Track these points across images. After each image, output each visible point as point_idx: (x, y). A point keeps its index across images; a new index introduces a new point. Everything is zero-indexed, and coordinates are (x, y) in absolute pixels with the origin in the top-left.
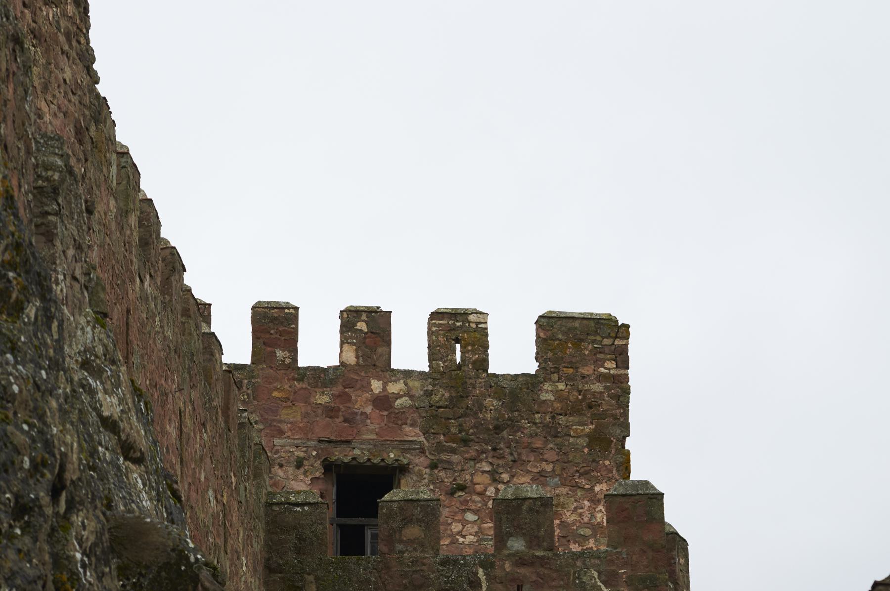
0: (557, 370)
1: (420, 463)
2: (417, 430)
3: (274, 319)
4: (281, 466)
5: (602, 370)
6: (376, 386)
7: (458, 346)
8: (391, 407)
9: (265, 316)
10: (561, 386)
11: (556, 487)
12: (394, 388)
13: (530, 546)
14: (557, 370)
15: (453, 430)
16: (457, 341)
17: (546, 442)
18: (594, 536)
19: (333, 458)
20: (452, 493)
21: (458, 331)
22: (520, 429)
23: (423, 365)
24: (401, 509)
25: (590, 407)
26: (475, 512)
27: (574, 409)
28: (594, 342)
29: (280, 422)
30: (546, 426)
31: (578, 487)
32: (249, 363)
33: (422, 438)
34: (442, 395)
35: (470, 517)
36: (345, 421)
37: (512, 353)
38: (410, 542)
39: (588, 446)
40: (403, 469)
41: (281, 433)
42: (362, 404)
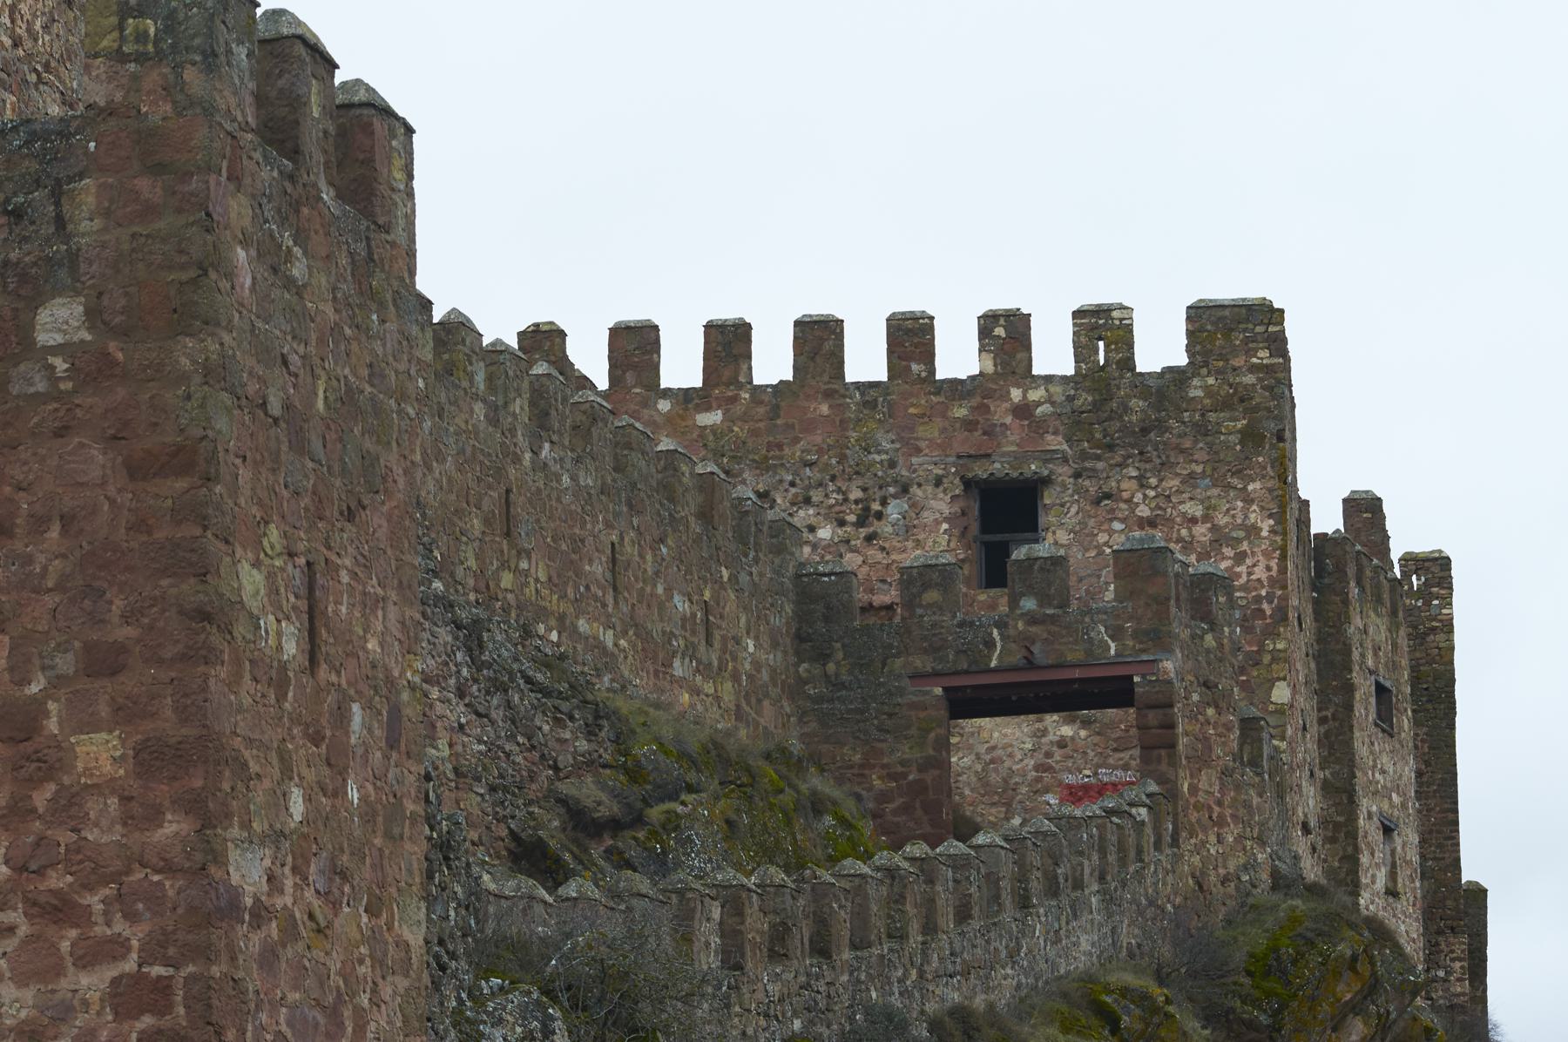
0: (1206, 364)
1: (1063, 473)
2: (1060, 438)
3: (908, 331)
4: (920, 485)
5: (1254, 360)
6: (1016, 394)
7: (1101, 344)
8: (1032, 415)
9: (899, 328)
10: (1211, 381)
11: (1207, 488)
12: (1034, 395)
13: (1041, 605)
14: (1206, 364)
15: (1098, 436)
16: (1100, 339)
17: (1196, 442)
18: (1248, 537)
19: (970, 475)
20: (1097, 502)
21: (1102, 327)
22: (1168, 429)
23: (1068, 368)
24: (920, 574)
25: (1242, 400)
26: (1123, 521)
27: (1225, 405)
28: (1245, 330)
29: (917, 439)
30: (1195, 425)
31: (1230, 486)
32: (884, 378)
33: (1065, 447)
34: (1085, 399)
35: (1117, 526)
36: (985, 433)
37: (1160, 347)
38: (930, 605)
39: (1241, 442)
40: (1046, 481)
41: (918, 450)
42: (1001, 415)
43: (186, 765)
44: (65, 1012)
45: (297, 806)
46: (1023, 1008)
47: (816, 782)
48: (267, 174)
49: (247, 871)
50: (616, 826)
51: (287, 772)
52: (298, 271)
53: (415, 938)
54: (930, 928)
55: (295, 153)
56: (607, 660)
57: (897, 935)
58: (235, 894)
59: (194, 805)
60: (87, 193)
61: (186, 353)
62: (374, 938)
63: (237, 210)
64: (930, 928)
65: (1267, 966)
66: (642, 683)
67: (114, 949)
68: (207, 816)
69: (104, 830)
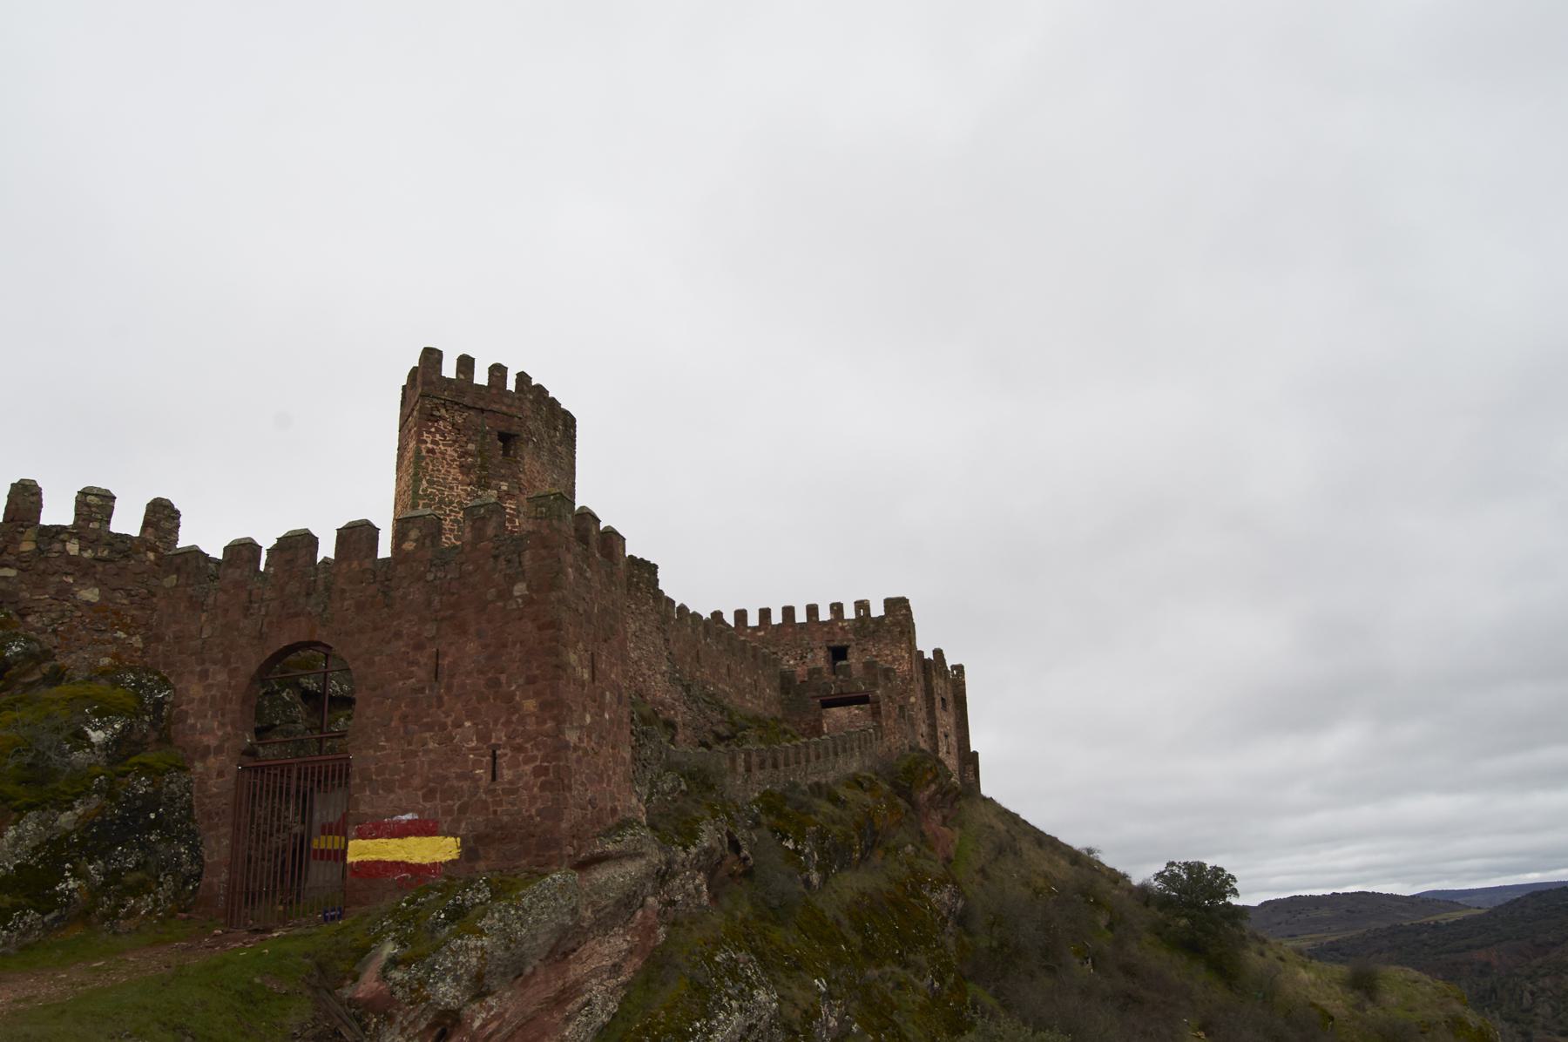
21: (862, 605)
23: (853, 616)
27: (894, 625)
37: (877, 610)
43: (554, 708)
44: (520, 777)
45: (588, 719)
46: (836, 782)
47: (785, 726)
48: (578, 549)
49: (572, 737)
50: (728, 738)
51: (585, 709)
52: (588, 575)
53: (628, 756)
54: (808, 761)
55: (587, 544)
56: (727, 695)
57: (798, 763)
58: (567, 743)
59: (554, 718)
60: (527, 555)
61: (553, 596)
62: (614, 756)
63: (569, 558)
64: (808, 761)
65: (908, 771)
66: (737, 701)
67: (534, 758)
68: (559, 722)
69: (531, 726)
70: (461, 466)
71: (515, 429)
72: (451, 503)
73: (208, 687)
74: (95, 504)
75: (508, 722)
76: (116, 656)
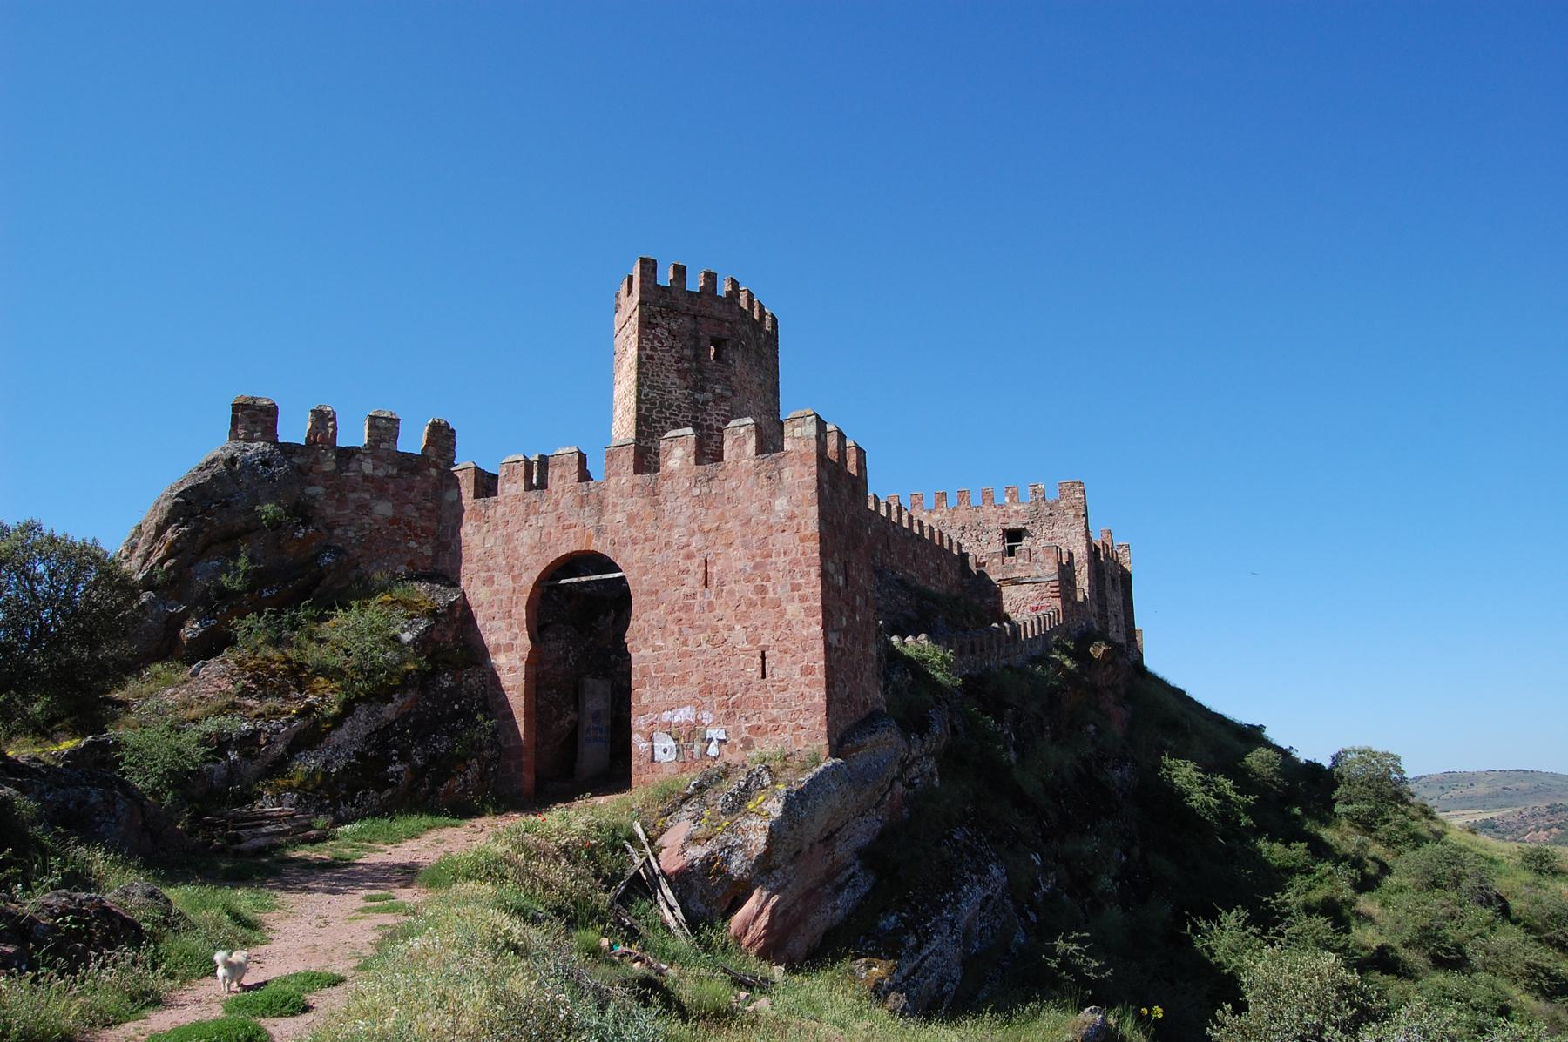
57: (991, 647)
62: (864, 654)
70: (678, 371)
71: (725, 334)
72: (671, 406)
73: (497, 593)
74: (384, 428)
75: (776, 626)
76: (410, 563)
